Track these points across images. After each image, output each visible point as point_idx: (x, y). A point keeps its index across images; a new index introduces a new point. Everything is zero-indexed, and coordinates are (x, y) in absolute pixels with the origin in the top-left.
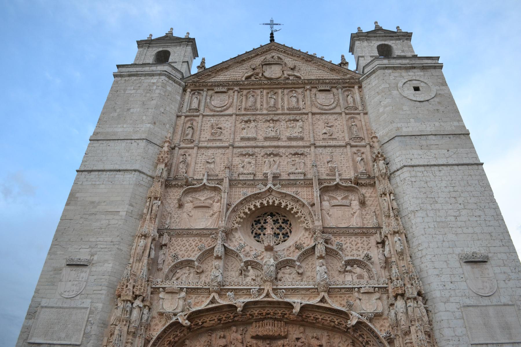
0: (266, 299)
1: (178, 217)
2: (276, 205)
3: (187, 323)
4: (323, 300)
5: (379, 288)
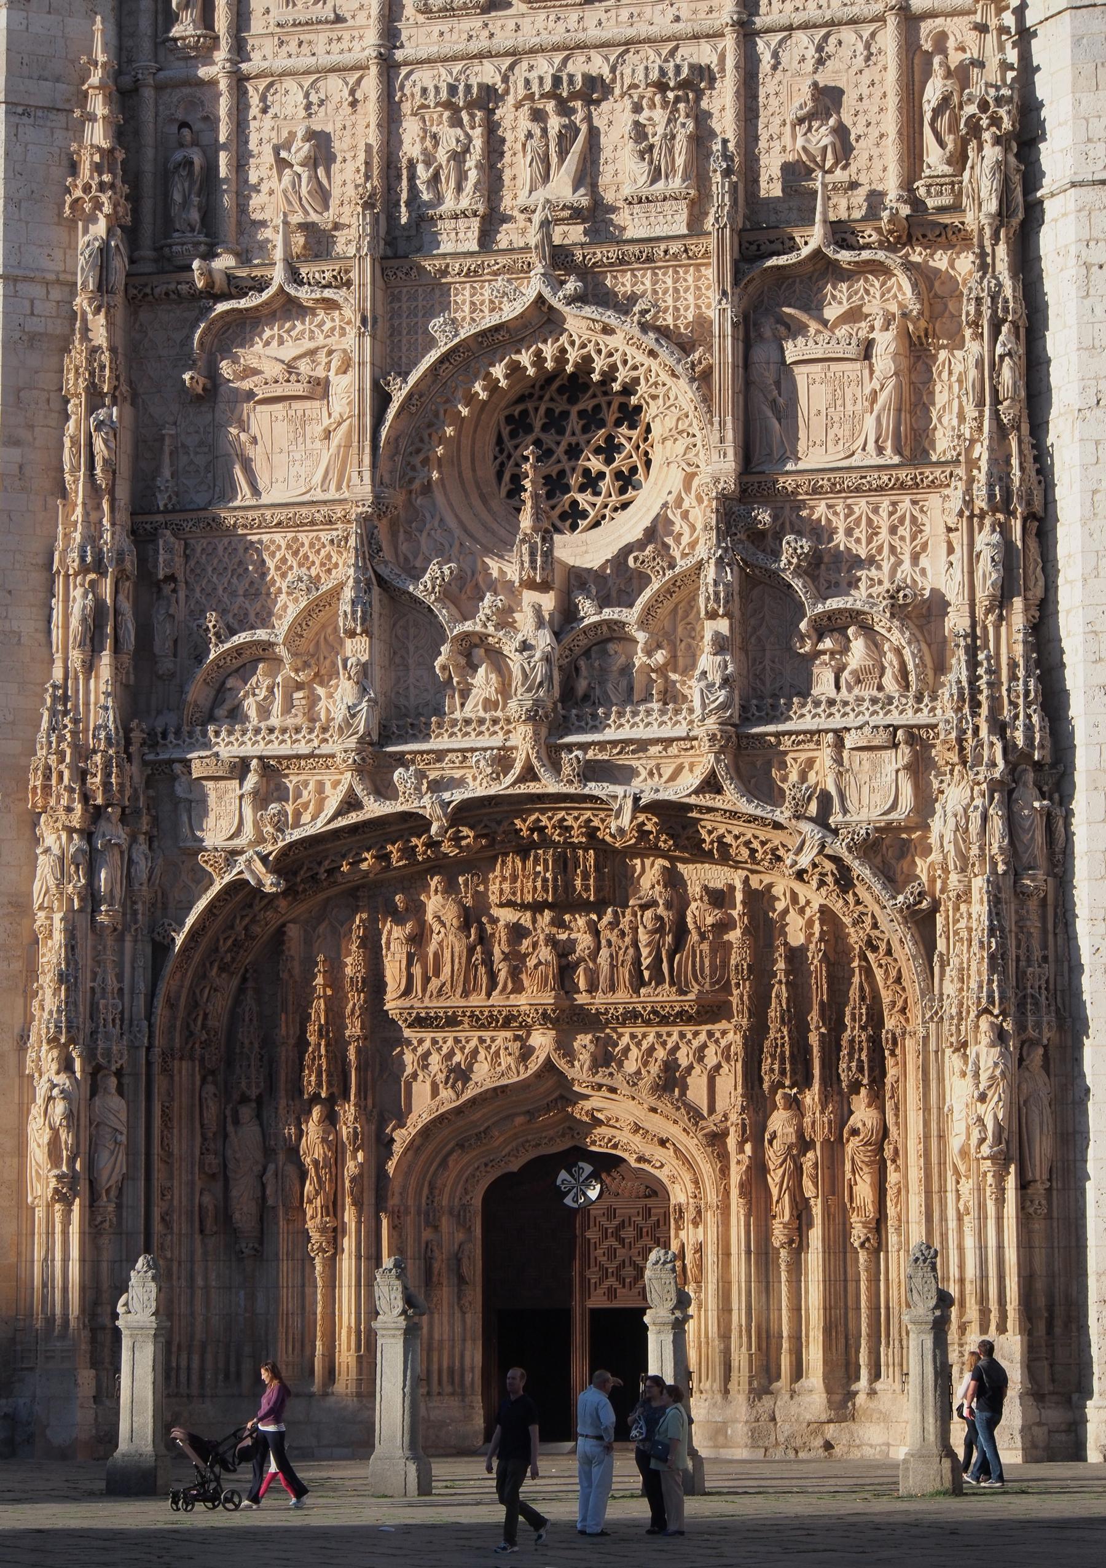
0: (522, 789)
1: (201, 444)
2: (569, 368)
3: (270, 883)
4: (711, 785)
5: (908, 728)
